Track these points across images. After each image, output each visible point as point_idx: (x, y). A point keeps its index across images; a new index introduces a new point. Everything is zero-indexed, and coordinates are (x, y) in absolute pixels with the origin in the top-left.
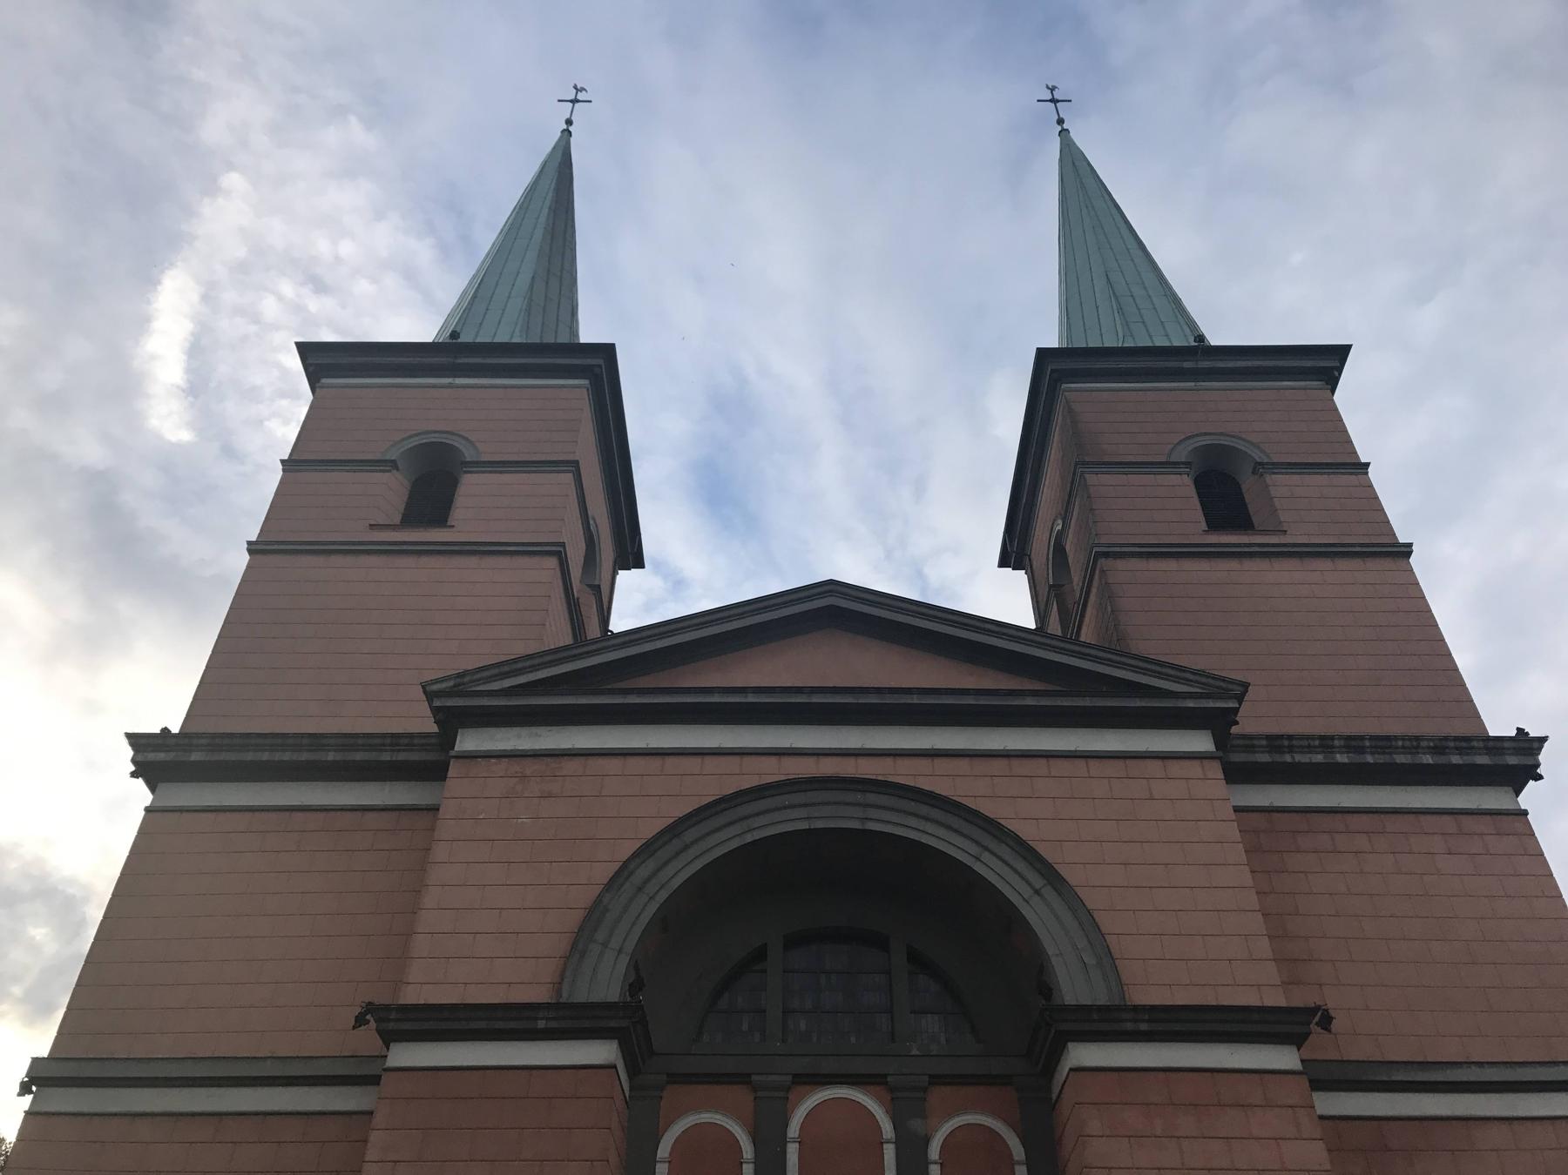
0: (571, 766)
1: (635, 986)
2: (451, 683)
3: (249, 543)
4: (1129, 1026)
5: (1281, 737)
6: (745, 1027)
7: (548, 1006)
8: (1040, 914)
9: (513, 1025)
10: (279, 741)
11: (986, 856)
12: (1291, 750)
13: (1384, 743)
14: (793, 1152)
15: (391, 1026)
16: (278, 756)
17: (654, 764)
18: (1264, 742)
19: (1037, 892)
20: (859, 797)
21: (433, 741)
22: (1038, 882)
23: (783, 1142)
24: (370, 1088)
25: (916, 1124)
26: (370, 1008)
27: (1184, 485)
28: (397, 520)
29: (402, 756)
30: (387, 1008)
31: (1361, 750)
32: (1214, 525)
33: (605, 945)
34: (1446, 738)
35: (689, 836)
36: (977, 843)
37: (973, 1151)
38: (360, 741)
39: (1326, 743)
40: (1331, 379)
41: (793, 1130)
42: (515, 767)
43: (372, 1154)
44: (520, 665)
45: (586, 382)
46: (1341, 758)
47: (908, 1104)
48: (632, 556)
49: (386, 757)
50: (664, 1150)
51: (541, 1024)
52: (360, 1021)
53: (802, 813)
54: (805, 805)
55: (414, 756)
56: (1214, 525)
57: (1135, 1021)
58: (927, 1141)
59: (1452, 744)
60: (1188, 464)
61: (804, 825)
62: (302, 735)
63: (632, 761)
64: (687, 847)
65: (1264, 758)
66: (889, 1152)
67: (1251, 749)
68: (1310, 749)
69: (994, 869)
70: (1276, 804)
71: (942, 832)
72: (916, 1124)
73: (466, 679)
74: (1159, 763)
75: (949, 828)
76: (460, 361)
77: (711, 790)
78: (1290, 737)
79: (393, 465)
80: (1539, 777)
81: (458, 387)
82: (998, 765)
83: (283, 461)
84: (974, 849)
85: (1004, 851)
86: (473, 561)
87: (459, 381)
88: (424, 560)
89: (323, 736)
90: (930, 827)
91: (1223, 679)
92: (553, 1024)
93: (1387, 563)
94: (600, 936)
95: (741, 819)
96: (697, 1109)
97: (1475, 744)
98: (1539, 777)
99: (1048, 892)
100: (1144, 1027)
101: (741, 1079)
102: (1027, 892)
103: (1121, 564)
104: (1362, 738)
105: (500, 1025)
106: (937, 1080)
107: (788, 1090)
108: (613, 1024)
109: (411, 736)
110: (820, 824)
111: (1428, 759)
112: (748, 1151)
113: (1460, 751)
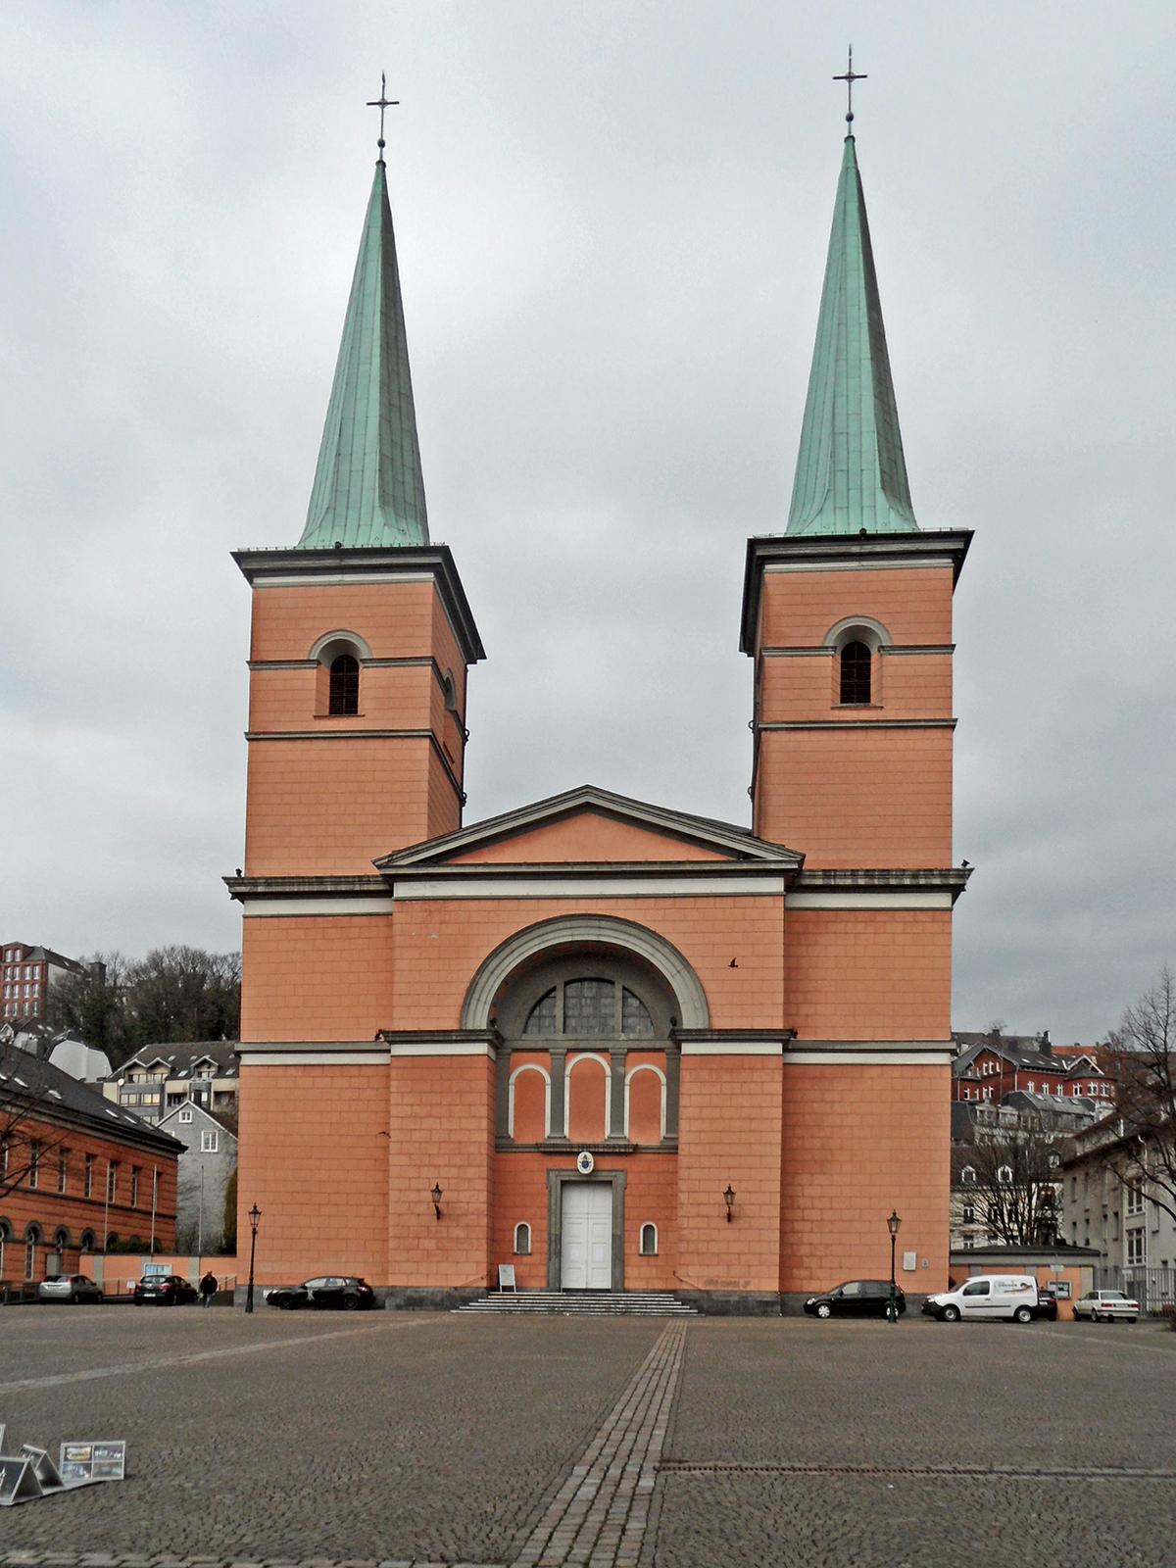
1: (492, 1022)
3: (246, 734)
4: (709, 1037)
5: (830, 871)
6: (547, 1024)
7: (456, 1031)
8: (679, 984)
9: (441, 1038)
10: (301, 880)
12: (835, 877)
13: (885, 873)
14: (567, 1081)
15: (390, 1039)
18: (820, 873)
19: (679, 972)
20: (597, 923)
21: (380, 879)
22: (680, 967)
24: (385, 1054)
25: (621, 1070)
26: (381, 1032)
27: (828, 668)
28: (327, 712)
30: (388, 1032)
31: (872, 877)
32: (842, 702)
33: (479, 1000)
34: (919, 870)
35: (514, 945)
36: (652, 946)
37: (646, 1081)
39: (854, 873)
41: (568, 1071)
42: (427, 905)
43: (393, 1089)
44: (420, 848)
45: (430, 576)
47: (619, 1059)
48: (473, 650)
50: (512, 1080)
51: (454, 1038)
52: (377, 1037)
53: (569, 932)
55: (373, 887)
56: (842, 702)
58: (625, 1076)
59: (922, 873)
60: (834, 648)
61: (570, 939)
62: (312, 878)
65: (819, 882)
66: (608, 1081)
67: (814, 877)
68: (845, 877)
70: (823, 906)
71: (637, 942)
74: (751, 899)
78: (835, 871)
79: (318, 662)
82: (669, 903)
83: (248, 662)
84: (651, 950)
85: (666, 951)
88: (351, 742)
90: (631, 939)
93: (938, 733)
94: (476, 996)
95: (539, 936)
96: (525, 1062)
97: (935, 873)
99: (684, 973)
100: (715, 1037)
101: (546, 1050)
102: (674, 971)
103: (774, 736)
104: (874, 870)
105: (436, 1038)
106: (630, 1050)
107: (566, 1055)
108: (486, 1038)
109: (368, 877)
111: (907, 882)
112: (548, 1080)
113: (926, 877)
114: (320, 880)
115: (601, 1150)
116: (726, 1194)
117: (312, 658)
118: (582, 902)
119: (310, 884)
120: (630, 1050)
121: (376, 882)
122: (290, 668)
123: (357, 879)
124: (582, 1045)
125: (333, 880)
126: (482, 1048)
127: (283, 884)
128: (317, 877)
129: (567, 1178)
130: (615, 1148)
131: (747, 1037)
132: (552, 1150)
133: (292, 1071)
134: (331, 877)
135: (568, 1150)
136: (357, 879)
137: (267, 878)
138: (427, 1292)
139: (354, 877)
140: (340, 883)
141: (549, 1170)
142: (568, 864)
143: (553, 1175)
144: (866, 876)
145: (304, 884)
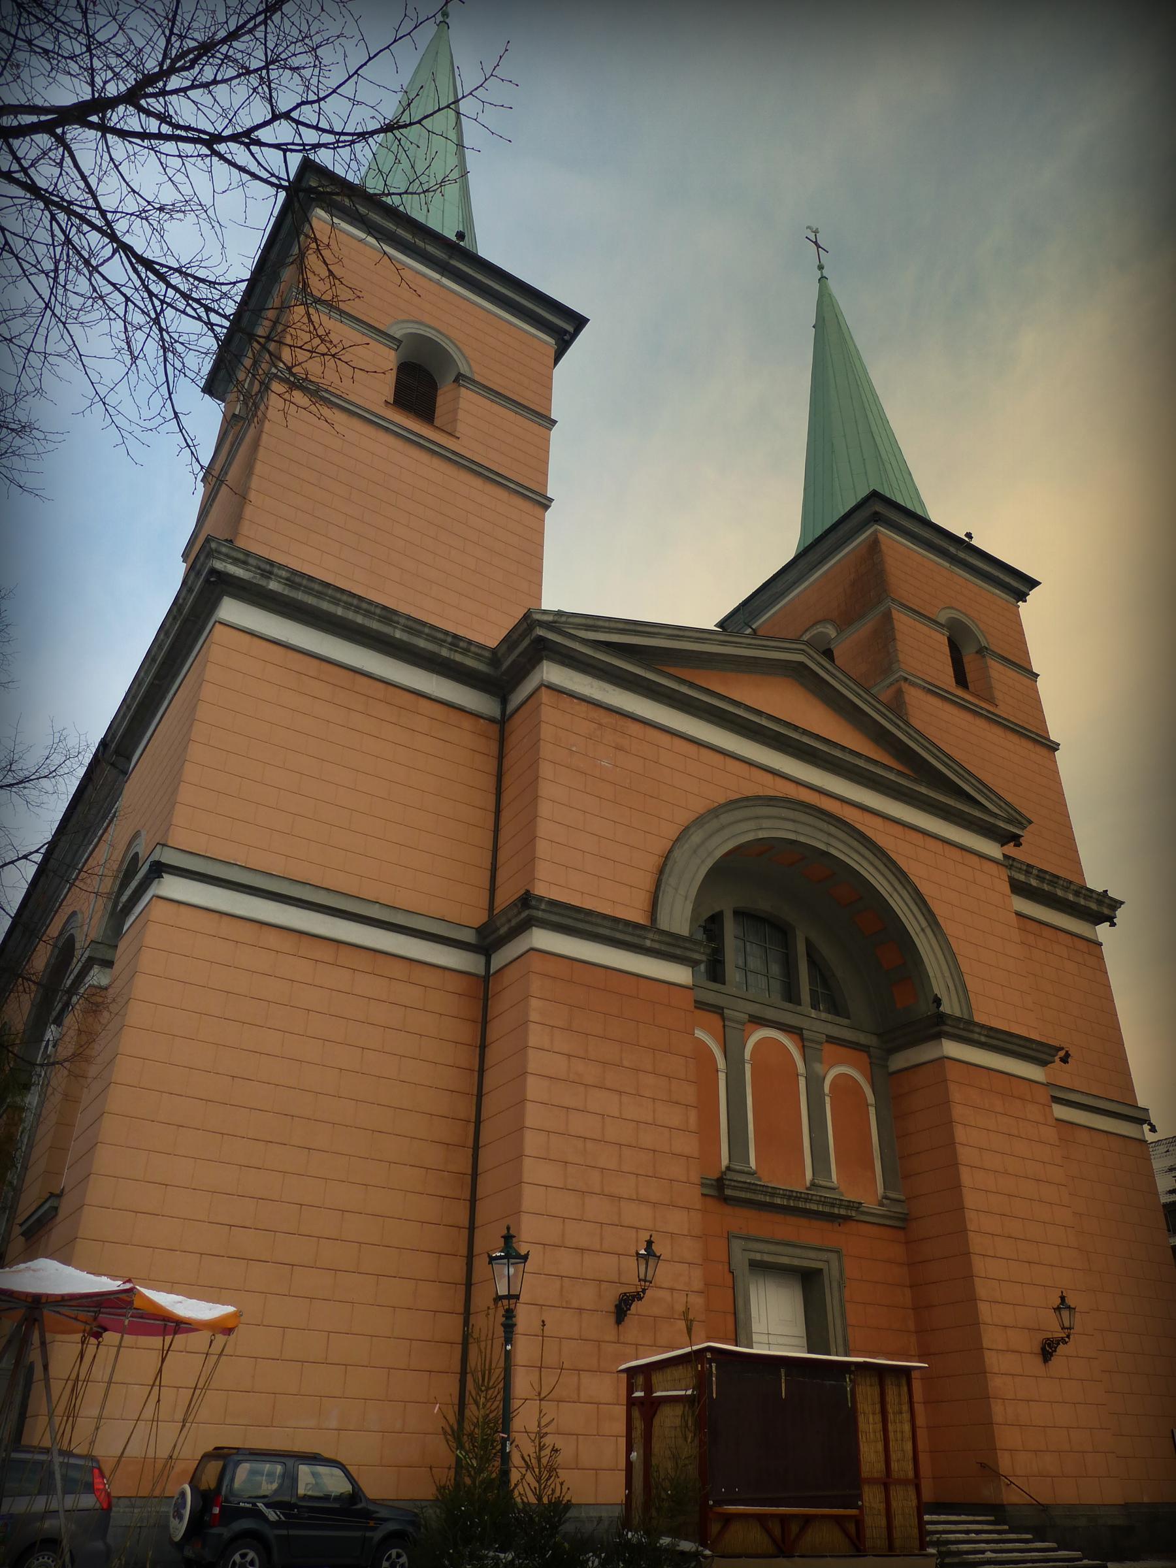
0: (635, 728)
2: (550, 618)
9: (628, 938)
10: (355, 602)
11: (895, 895)
16: (351, 615)
17: (691, 749)
21: (487, 654)
22: (924, 924)
23: (743, 1062)
25: (819, 1068)
29: (458, 658)
38: (427, 630)
40: (1022, 597)
41: (747, 1055)
46: (1034, 882)
49: (445, 652)
51: (648, 943)
53: (790, 826)
54: (794, 821)
55: (469, 662)
57: (980, 1034)
62: (377, 605)
63: (677, 742)
64: (723, 828)
66: (802, 1082)
69: (901, 905)
72: (819, 1068)
73: (563, 619)
75: (877, 868)
76: (453, 262)
77: (750, 790)
80: (1113, 925)
81: (443, 286)
86: (477, 483)
87: (445, 281)
89: (395, 612)
91: (1019, 813)
92: (656, 946)
93: (1044, 752)
98: (1113, 925)
100: (983, 1039)
102: (918, 929)
105: (618, 936)
106: (831, 1040)
107: (744, 1024)
109: (470, 642)
110: (802, 839)
112: (721, 1064)
114: (388, 615)
115: (814, 1207)
116: (1057, 1309)
117: (391, 332)
118: (802, 790)
119: (368, 614)
120: (831, 1040)
121: (478, 657)
122: (358, 331)
123: (449, 639)
124: (770, 1014)
125: (410, 623)
126: (679, 974)
127: (319, 595)
128: (385, 608)
129: (758, 1257)
130: (833, 1205)
131: (1015, 1048)
132: (743, 1195)
133: (272, 939)
134: (409, 618)
135: (768, 1199)
136: (449, 639)
137: (295, 572)
138: (600, 1520)
139: (446, 633)
140: (418, 633)
141: (730, 1237)
142: (796, 728)
143: (737, 1245)
144: (1038, 877)
145: (357, 610)
